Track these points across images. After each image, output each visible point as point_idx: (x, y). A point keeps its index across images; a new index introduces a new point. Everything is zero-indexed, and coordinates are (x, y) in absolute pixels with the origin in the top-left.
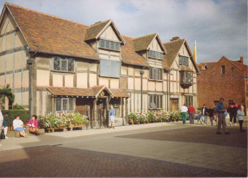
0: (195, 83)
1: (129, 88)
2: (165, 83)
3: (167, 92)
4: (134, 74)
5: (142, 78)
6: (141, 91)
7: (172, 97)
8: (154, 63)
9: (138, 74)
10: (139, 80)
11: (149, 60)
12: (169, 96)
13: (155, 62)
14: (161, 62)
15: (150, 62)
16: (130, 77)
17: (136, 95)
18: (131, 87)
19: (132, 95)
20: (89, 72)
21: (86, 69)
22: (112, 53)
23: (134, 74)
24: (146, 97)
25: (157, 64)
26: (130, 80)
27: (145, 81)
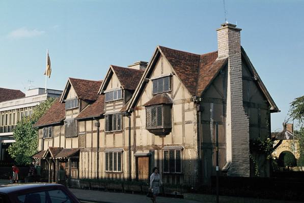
0: (189, 122)
1: (87, 147)
2: (127, 132)
3: (130, 147)
4: (92, 129)
5: (98, 132)
6: (97, 150)
7: (139, 152)
8: (112, 108)
9: (95, 129)
10: (95, 135)
11: (107, 105)
12: (132, 152)
13: (114, 106)
14: (122, 103)
15: (107, 108)
16: (88, 132)
17: (93, 153)
18: (89, 145)
19: (90, 153)
20: (60, 135)
21: (59, 133)
22: (75, 111)
23: (92, 129)
24: (103, 156)
25: (116, 107)
26: (89, 136)
27: (102, 135)
